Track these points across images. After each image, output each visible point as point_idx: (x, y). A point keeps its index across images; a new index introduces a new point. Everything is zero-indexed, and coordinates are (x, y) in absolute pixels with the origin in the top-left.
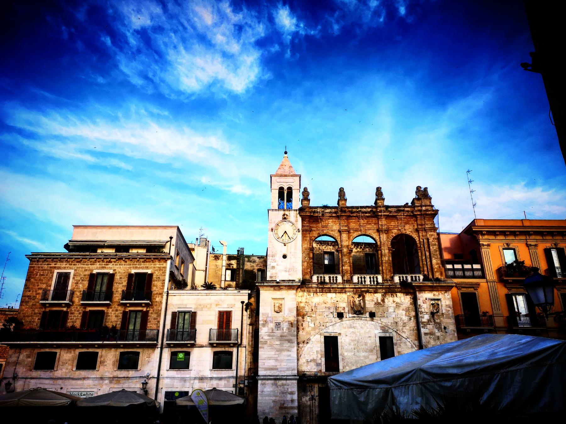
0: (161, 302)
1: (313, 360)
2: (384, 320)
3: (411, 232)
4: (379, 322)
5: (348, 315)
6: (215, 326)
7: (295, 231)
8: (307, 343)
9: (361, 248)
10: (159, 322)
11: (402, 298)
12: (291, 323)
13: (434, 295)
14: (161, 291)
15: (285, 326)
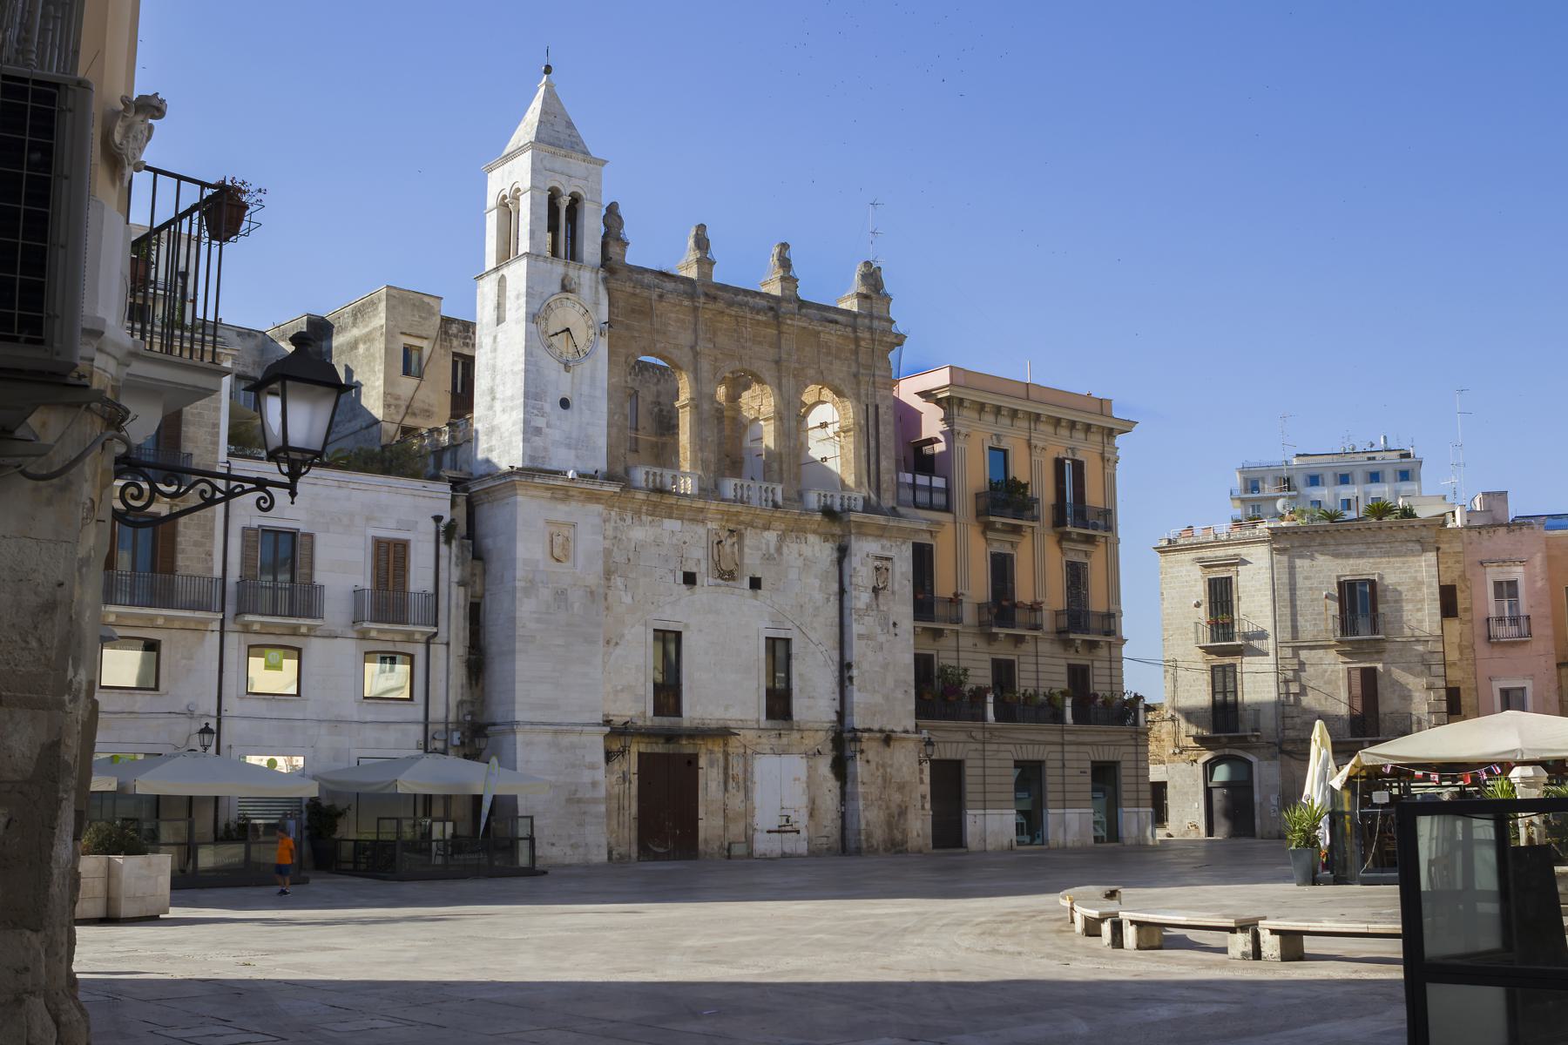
6: (365, 580)
10: (210, 554)
11: (817, 548)
12: (592, 593)
13: (883, 547)
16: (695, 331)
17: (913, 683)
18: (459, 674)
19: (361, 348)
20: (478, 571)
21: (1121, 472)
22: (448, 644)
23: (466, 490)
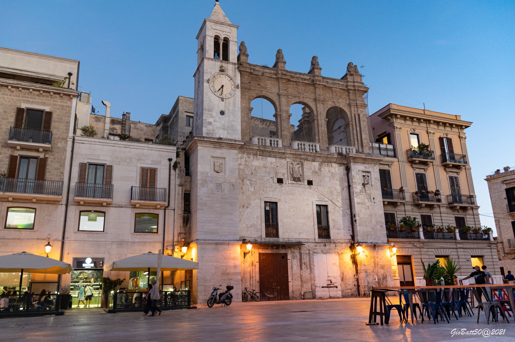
0: (65, 150)
1: (253, 226)
2: (321, 189)
3: (344, 106)
4: (316, 190)
5: (287, 181)
6: (136, 183)
7: (233, 87)
8: (247, 207)
9: (266, 125)
10: (62, 173)
11: (337, 169)
12: (233, 185)
13: (366, 167)
14: (64, 136)
16: (279, 87)
17: (384, 223)
18: (179, 222)
20: (189, 180)
21: (468, 142)
22: (174, 210)
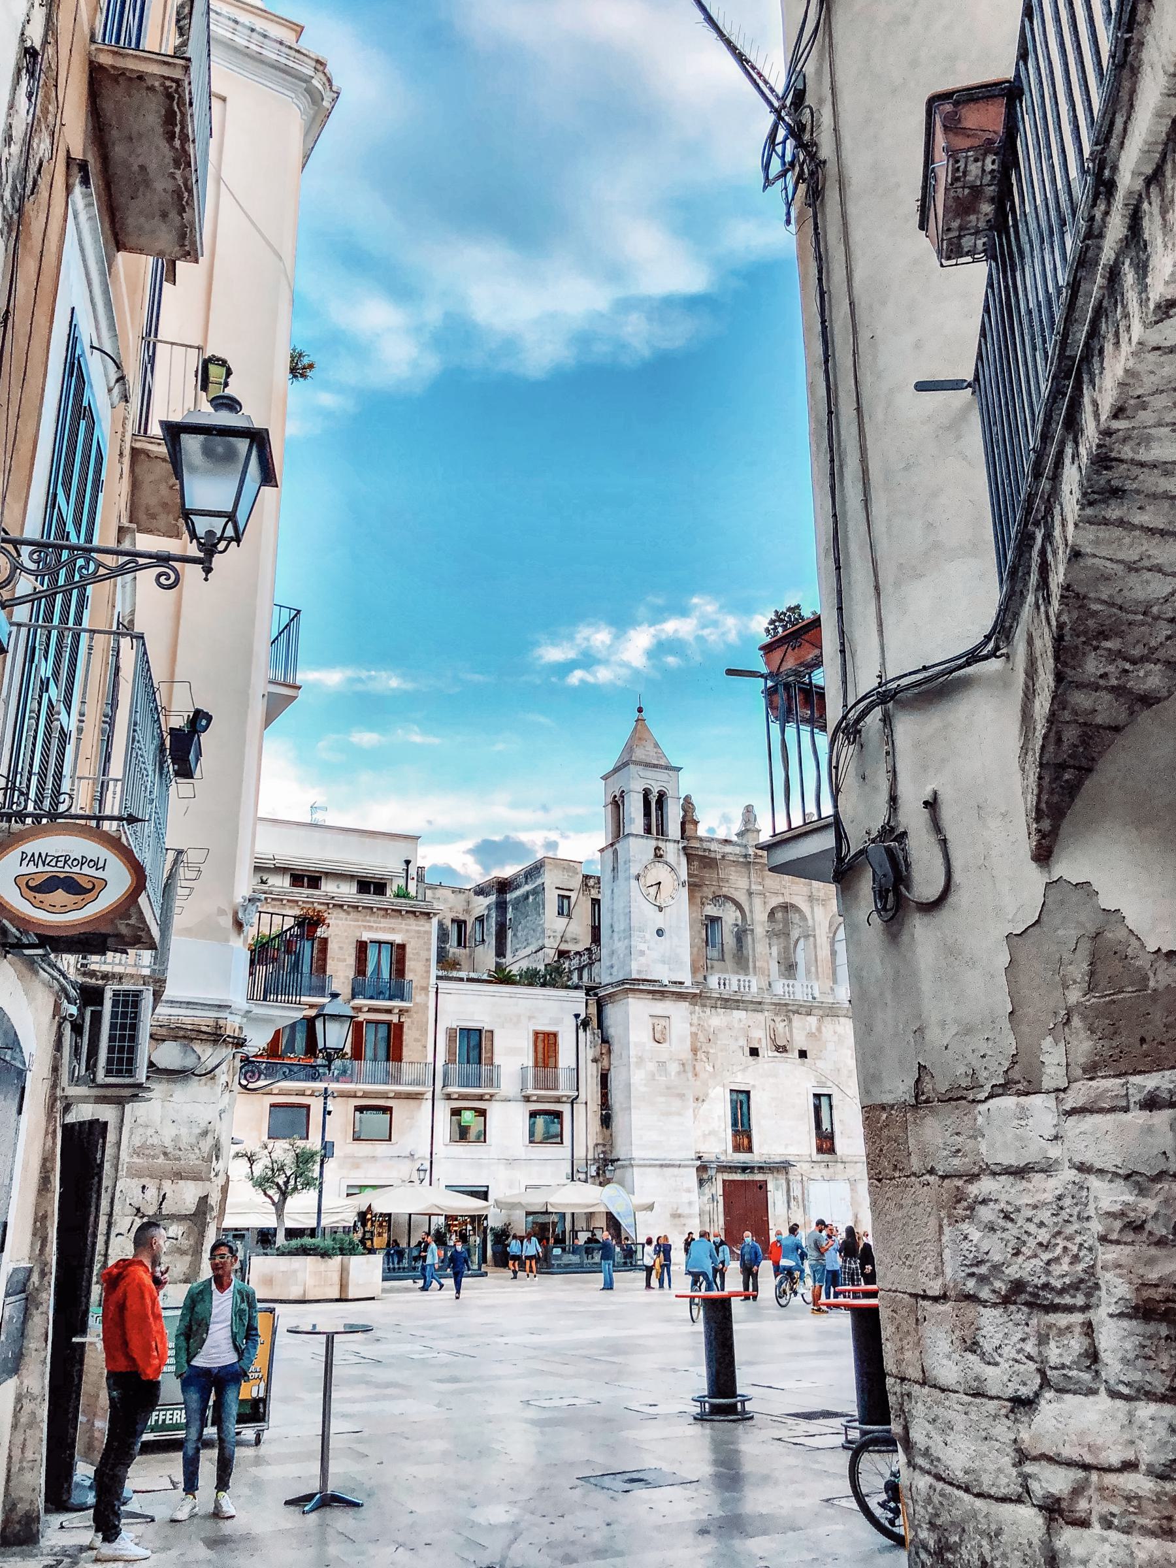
2: (819, 1064)
5: (766, 1052)
15: (674, 1068)
19: (531, 898)
23: (596, 994)
